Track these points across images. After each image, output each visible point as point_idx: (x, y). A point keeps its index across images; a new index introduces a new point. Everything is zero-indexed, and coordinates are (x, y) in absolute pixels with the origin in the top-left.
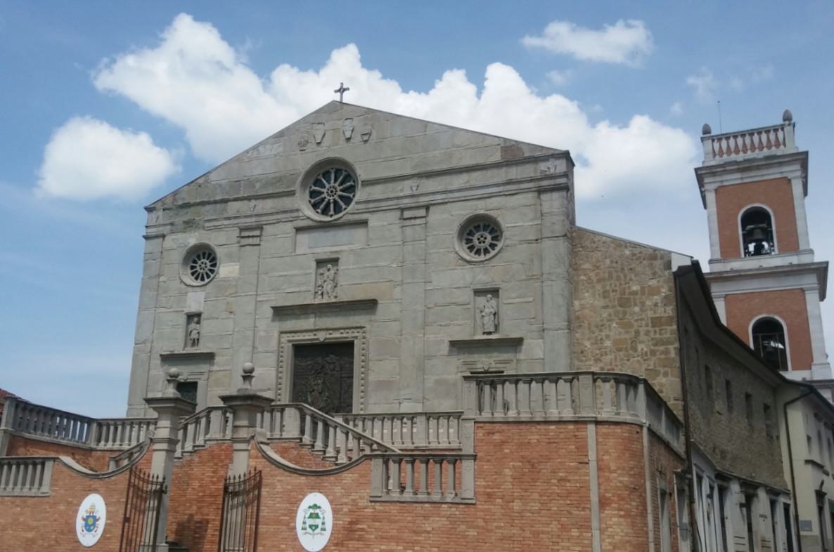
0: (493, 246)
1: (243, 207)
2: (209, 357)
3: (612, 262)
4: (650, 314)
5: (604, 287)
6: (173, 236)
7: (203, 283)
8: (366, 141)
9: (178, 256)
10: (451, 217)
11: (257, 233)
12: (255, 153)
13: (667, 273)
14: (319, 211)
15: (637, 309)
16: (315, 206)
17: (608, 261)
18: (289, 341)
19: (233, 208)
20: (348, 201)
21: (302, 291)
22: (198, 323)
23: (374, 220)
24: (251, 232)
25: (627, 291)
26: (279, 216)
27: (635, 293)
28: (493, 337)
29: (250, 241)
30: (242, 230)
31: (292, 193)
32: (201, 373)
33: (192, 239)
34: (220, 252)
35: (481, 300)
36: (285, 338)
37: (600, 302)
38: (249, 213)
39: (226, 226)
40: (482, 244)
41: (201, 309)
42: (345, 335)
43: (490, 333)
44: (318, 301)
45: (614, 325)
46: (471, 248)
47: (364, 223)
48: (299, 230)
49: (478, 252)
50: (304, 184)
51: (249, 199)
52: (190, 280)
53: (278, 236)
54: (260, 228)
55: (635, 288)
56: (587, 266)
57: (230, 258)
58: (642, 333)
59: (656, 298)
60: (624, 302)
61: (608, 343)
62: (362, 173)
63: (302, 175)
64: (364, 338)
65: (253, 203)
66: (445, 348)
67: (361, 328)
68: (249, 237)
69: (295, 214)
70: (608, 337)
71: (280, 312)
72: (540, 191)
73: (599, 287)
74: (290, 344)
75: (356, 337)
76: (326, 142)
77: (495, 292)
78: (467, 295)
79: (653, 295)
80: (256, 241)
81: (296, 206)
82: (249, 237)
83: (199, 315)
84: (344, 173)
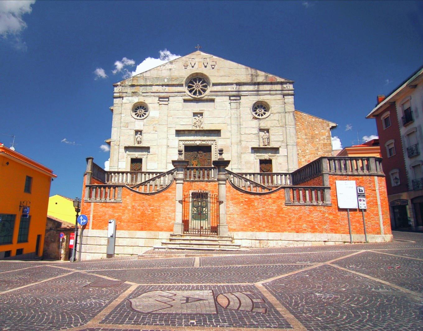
0: (264, 114)
1: (160, 89)
2: (147, 149)
3: (308, 123)
4: (322, 142)
5: (305, 131)
6: (127, 98)
7: (140, 118)
8: (213, 68)
9: (130, 106)
10: (248, 101)
11: (167, 100)
12: (164, 68)
13: (328, 128)
14: (192, 93)
15: (317, 140)
16: (190, 91)
17: (306, 123)
18: (183, 144)
19: (155, 89)
20: (204, 91)
21: (188, 123)
22: (141, 134)
23: (217, 99)
24: (164, 99)
25: (314, 134)
26: (176, 94)
27: (317, 134)
28: (267, 146)
29: (164, 103)
30: (160, 98)
31: (181, 85)
32: (144, 155)
33: (136, 100)
34: (150, 106)
35: (262, 134)
36: (181, 143)
37: (304, 137)
38: (163, 91)
39: (151, 96)
40: (260, 112)
41: (142, 129)
42: (208, 143)
43: (266, 145)
44: (195, 128)
45: (310, 145)
46: (256, 114)
47: (212, 101)
48: (185, 101)
49: (259, 115)
50: (186, 83)
51: (162, 85)
52: (135, 117)
53: (176, 102)
54: (168, 98)
55: (317, 132)
56: (298, 124)
57: (154, 108)
58: (320, 148)
59: (324, 137)
60: (313, 137)
61: (307, 151)
62: (213, 80)
63: (186, 78)
64: (216, 144)
65: (164, 87)
66: (250, 150)
67: (215, 140)
68: (163, 101)
69: (184, 94)
70: (307, 149)
71: (179, 133)
72: (284, 95)
73: (303, 131)
74: (184, 145)
75: (212, 144)
76: (196, 66)
77: (268, 131)
78: (256, 131)
79: (323, 135)
80: (166, 103)
81: (184, 90)
82: (163, 101)
83: (141, 131)
84: (203, 80)
